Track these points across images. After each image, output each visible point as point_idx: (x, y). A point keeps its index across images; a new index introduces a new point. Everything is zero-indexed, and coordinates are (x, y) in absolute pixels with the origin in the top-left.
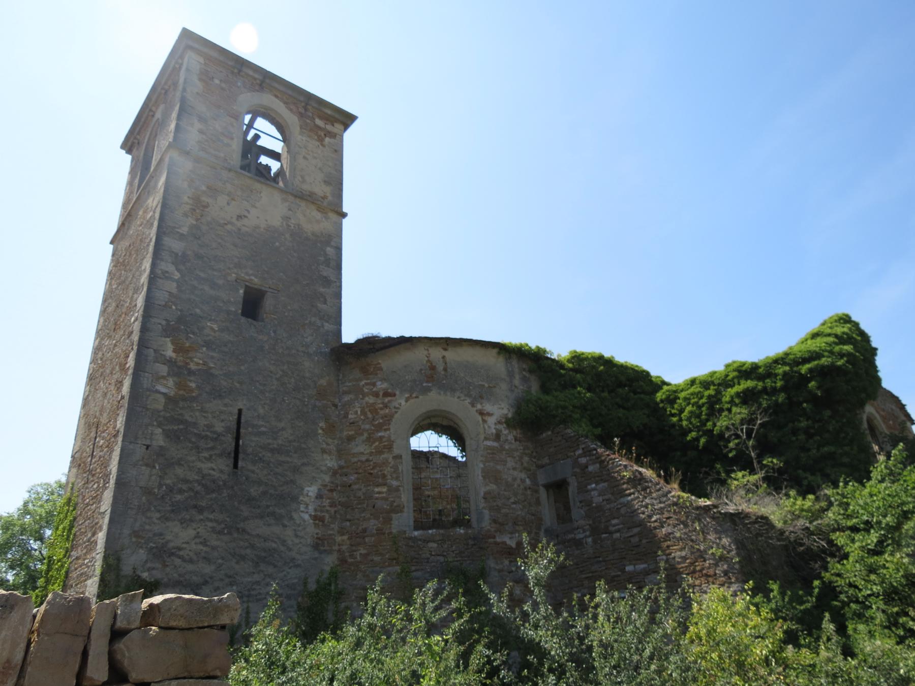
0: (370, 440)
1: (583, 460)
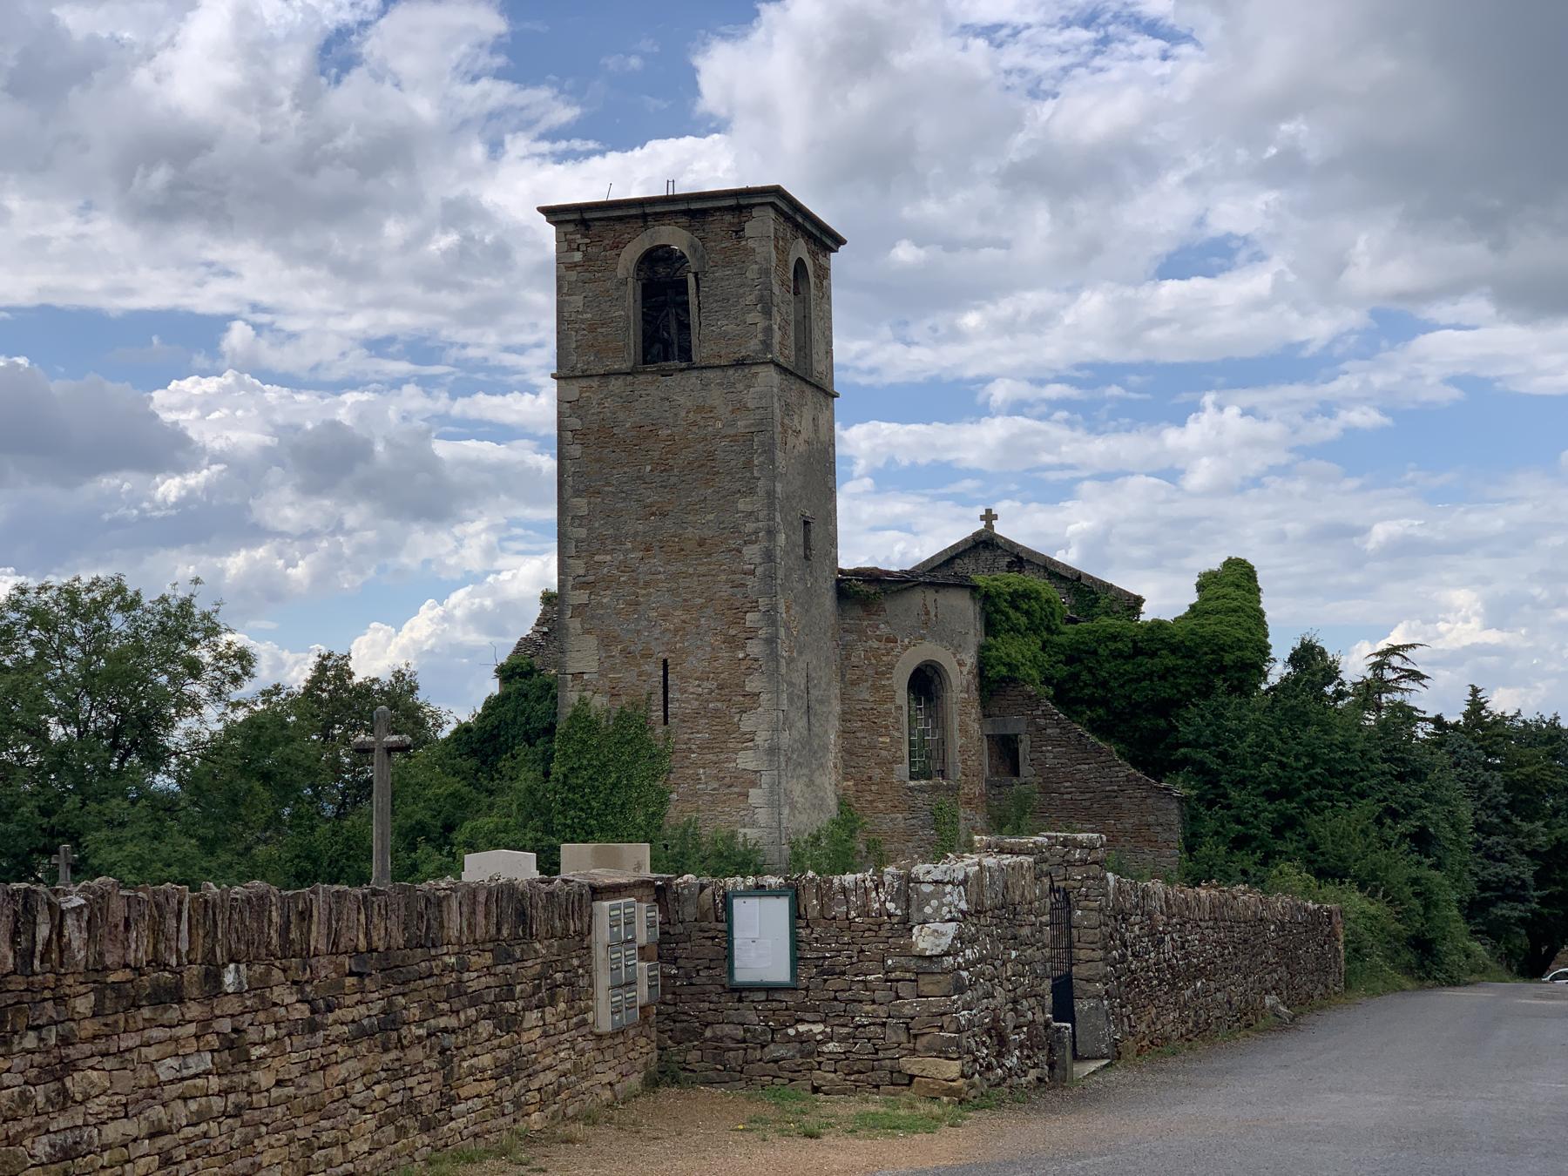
0: (875, 688)
1: (1042, 722)
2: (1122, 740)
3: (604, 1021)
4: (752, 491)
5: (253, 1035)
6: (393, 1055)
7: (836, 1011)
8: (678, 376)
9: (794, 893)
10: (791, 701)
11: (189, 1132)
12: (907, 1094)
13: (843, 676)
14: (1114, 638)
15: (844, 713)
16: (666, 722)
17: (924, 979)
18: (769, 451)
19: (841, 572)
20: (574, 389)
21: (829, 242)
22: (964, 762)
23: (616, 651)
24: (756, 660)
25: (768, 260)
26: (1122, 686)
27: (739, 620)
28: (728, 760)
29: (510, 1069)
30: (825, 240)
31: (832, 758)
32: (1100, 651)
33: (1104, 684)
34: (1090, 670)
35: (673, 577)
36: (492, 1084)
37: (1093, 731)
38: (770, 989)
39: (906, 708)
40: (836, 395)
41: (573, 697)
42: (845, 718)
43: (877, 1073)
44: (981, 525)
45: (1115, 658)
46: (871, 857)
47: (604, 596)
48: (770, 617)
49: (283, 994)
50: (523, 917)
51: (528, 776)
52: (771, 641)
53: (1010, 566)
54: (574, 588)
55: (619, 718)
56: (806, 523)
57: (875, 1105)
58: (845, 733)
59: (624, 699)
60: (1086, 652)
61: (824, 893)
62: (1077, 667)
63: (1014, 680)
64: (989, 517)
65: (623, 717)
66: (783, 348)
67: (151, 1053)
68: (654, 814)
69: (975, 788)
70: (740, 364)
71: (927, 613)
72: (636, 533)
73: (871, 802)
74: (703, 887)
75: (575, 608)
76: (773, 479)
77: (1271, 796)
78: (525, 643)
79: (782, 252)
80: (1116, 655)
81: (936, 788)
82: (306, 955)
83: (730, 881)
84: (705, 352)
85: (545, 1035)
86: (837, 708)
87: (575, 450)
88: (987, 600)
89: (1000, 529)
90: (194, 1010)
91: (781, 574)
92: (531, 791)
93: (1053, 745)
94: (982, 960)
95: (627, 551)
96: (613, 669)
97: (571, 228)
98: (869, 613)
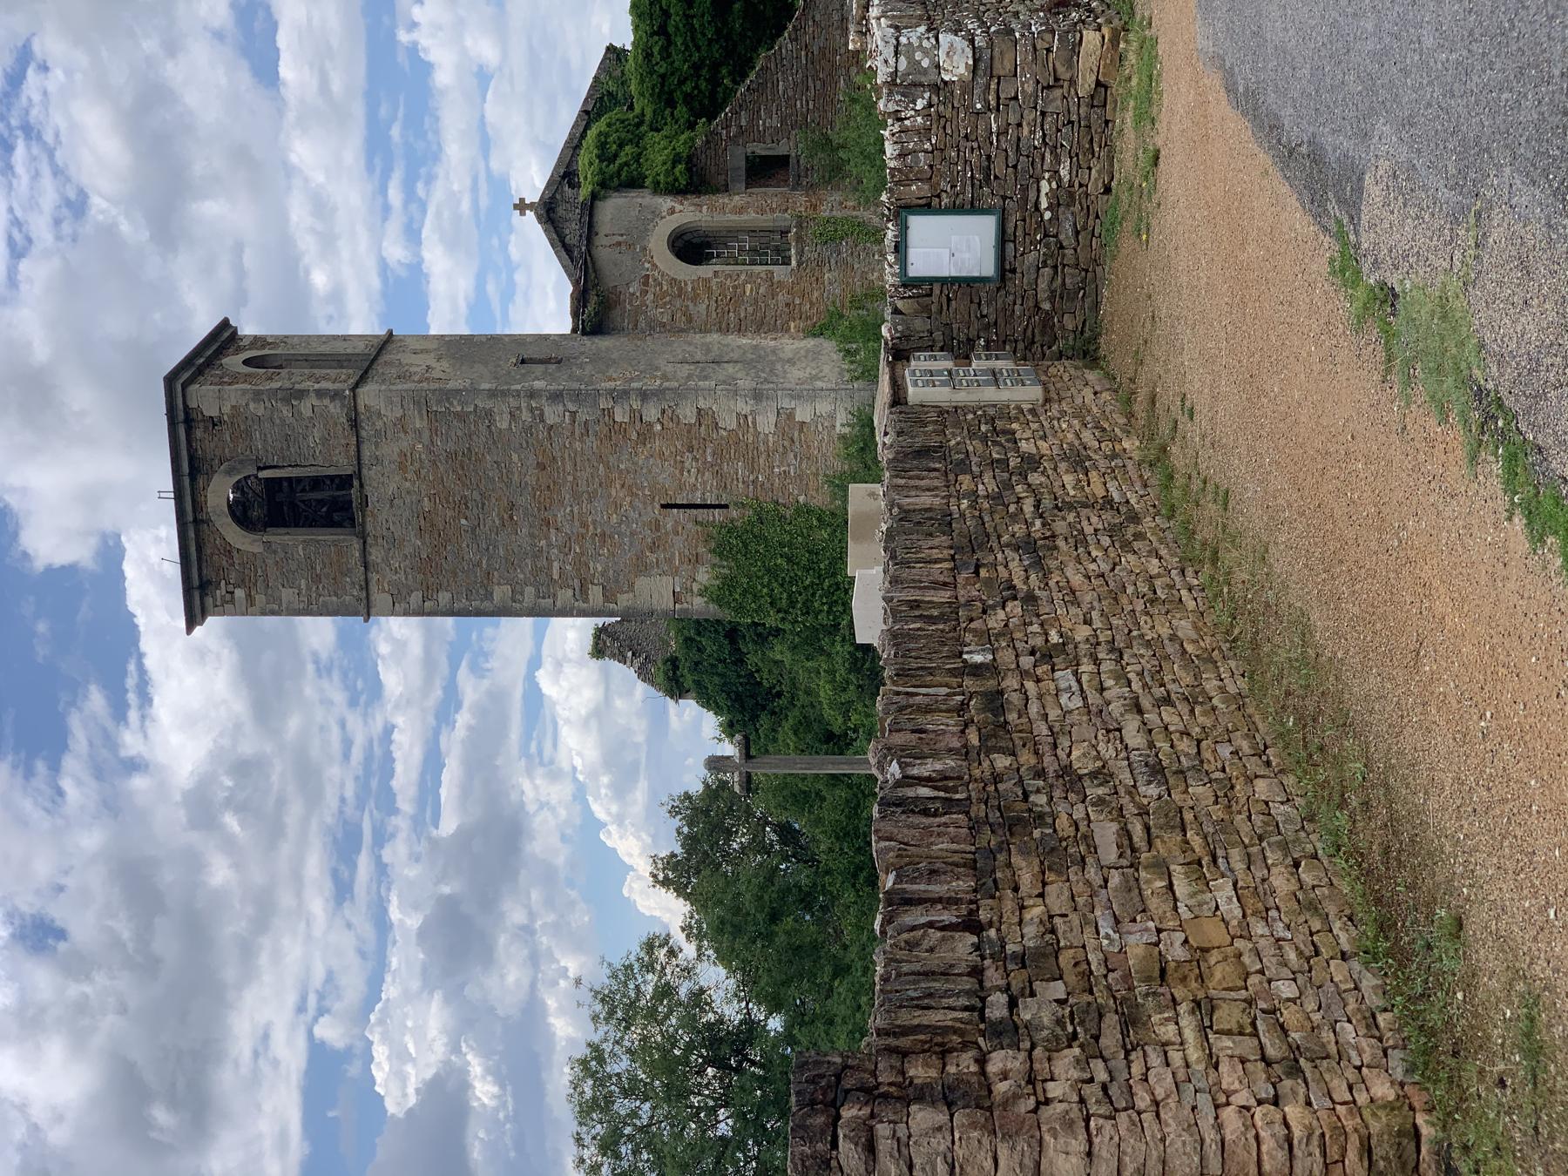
0: (695, 298)
2: (755, 50)
3: (1033, 393)
4: (489, 414)
5: (1038, 641)
6: (1060, 543)
7: (1027, 170)
8: (368, 490)
9: (903, 210)
10: (706, 378)
11: (1136, 686)
12: (1116, 89)
13: (682, 330)
14: (648, 56)
15: (720, 330)
16: (726, 506)
17: (998, 70)
18: (447, 395)
19: (574, 330)
20: (380, 598)
21: (226, 335)
22: (772, 210)
23: (652, 558)
24: (663, 412)
25: (244, 392)
26: (698, 49)
27: (622, 429)
28: (766, 442)
29: (1078, 460)
30: (223, 338)
31: (767, 342)
32: (662, 71)
33: (697, 67)
34: (682, 82)
35: (576, 496)
36: (1093, 475)
37: (744, 76)
38: (1003, 238)
39: (717, 268)
40: (390, 334)
41: (698, 602)
42: (725, 330)
43: (1093, 120)
44: (530, 214)
45: (669, 56)
46: (869, 306)
47: (595, 569)
48: (620, 396)
49: (996, 620)
50: (923, 452)
51: (779, 651)
52: (644, 396)
53: (572, 186)
54: (586, 600)
55: (721, 555)
56: (523, 362)
57: (1126, 120)
58: (740, 330)
59: (701, 550)
60: (663, 85)
61: (905, 176)
62: (678, 95)
63: (690, 158)
64: (522, 207)
65: (721, 551)
66: (340, 380)
67: (1053, 714)
68: (819, 520)
69: (800, 200)
70: (355, 424)
71: (619, 244)
72: (532, 535)
73: (812, 304)
74: (896, 311)
75: (607, 598)
76: (474, 391)
78: (643, 674)
79: (235, 378)
80: (666, 53)
81: (799, 239)
82: (954, 605)
83: (890, 280)
84: (343, 460)
85: (1044, 438)
86: (715, 336)
87: (444, 598)
88: (606, 185)
89: (533, 197)
90: (1011, 682)
91: (576, 385)
92: (793, 648)
93: (761, 118)
94: (979, 19)
95: (549, 545)
96: (670, 561)
97: (209, 601)
98: (618, 302)
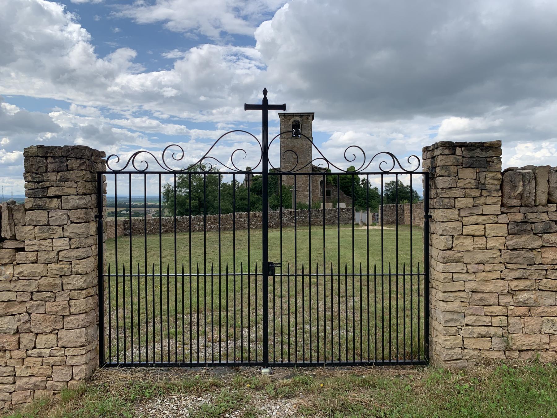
20: (283, 140)
77: (364, 199)
87: (283, 149)
